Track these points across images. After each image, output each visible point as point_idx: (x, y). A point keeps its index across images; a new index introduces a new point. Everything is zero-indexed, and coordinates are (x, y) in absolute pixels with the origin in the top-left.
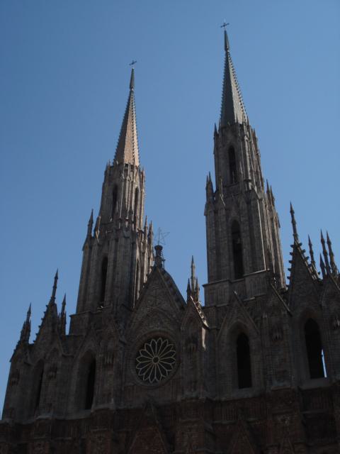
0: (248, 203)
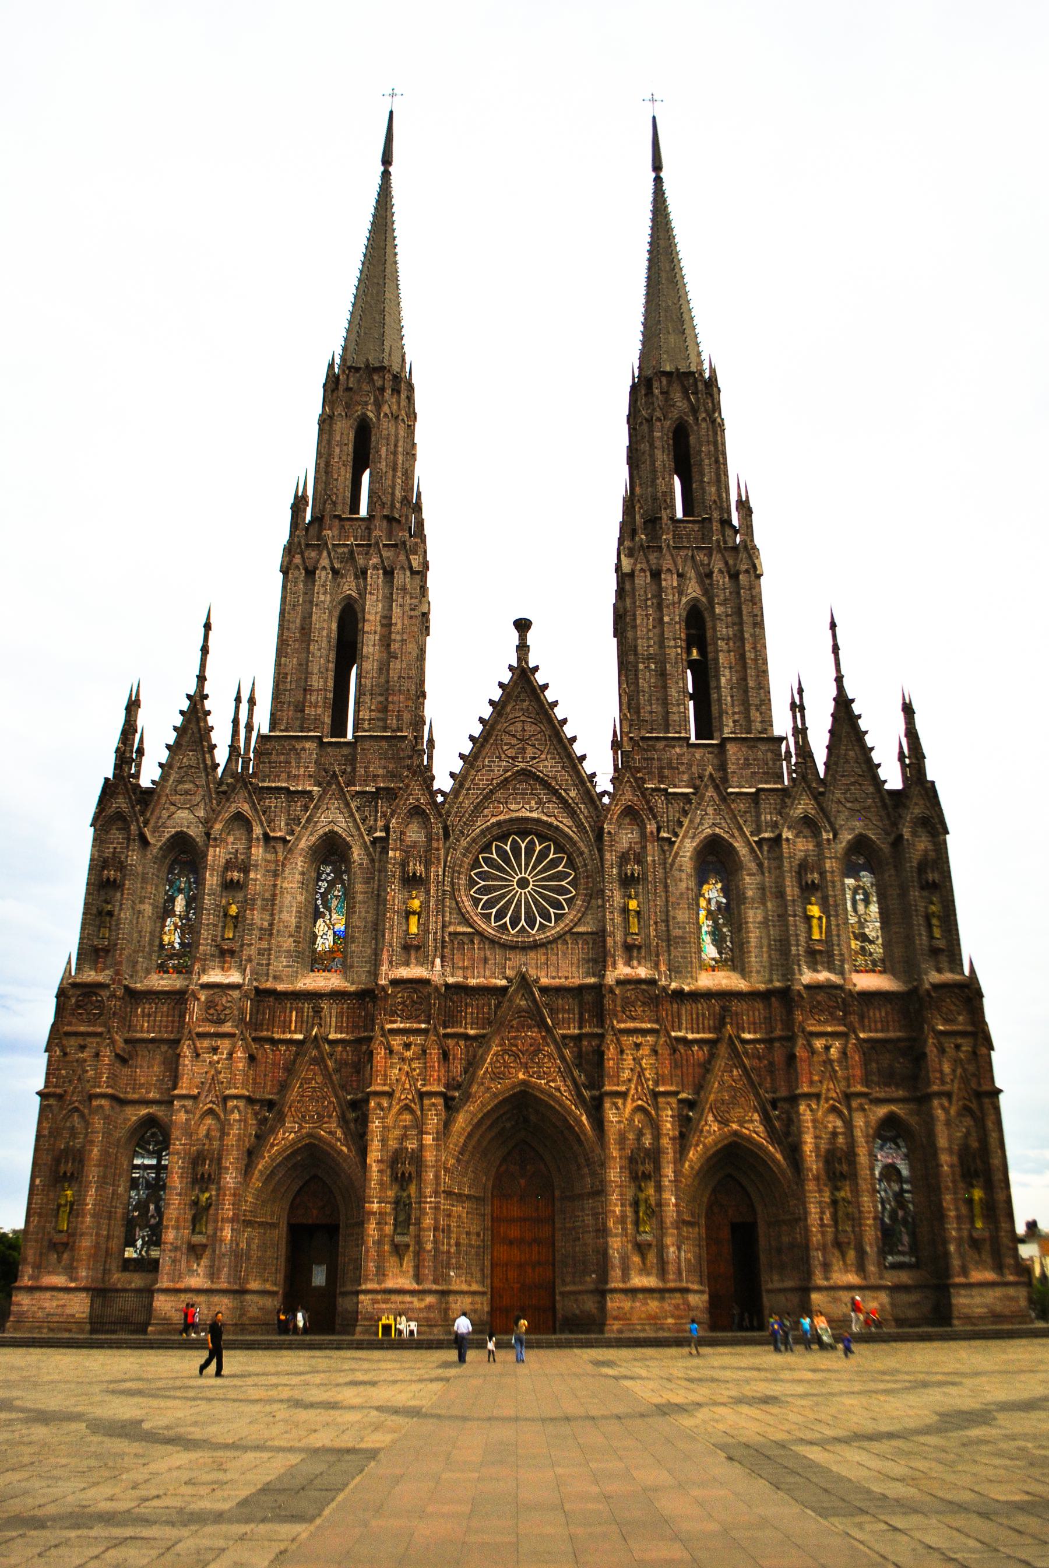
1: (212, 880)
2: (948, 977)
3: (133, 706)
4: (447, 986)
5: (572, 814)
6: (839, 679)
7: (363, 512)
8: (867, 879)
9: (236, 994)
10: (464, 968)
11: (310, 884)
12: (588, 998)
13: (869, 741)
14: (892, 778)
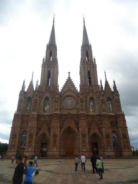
0: (93, 67)
1: (33, 102)
2: (120, 113)
3: (24, 82)
4: (60, 114)
6: (106, 79)
7: (51, 61)
8: (110, 102)
9: (35, 115)
10: (62, 112)
11: (44, 102)
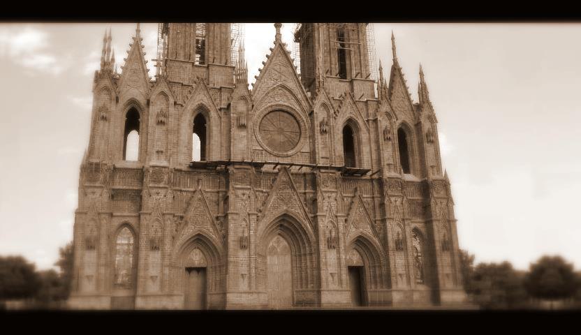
5: (300, 105)
12: (308, 178)
13: (407, 84)
14: (415, 99)
